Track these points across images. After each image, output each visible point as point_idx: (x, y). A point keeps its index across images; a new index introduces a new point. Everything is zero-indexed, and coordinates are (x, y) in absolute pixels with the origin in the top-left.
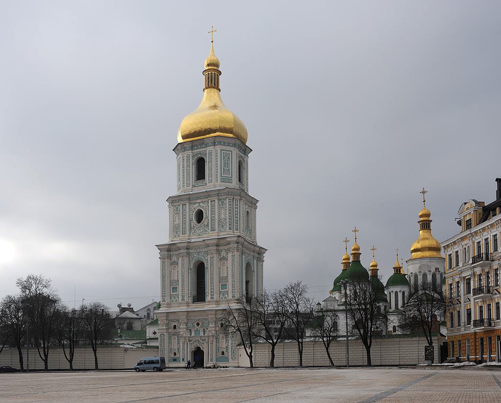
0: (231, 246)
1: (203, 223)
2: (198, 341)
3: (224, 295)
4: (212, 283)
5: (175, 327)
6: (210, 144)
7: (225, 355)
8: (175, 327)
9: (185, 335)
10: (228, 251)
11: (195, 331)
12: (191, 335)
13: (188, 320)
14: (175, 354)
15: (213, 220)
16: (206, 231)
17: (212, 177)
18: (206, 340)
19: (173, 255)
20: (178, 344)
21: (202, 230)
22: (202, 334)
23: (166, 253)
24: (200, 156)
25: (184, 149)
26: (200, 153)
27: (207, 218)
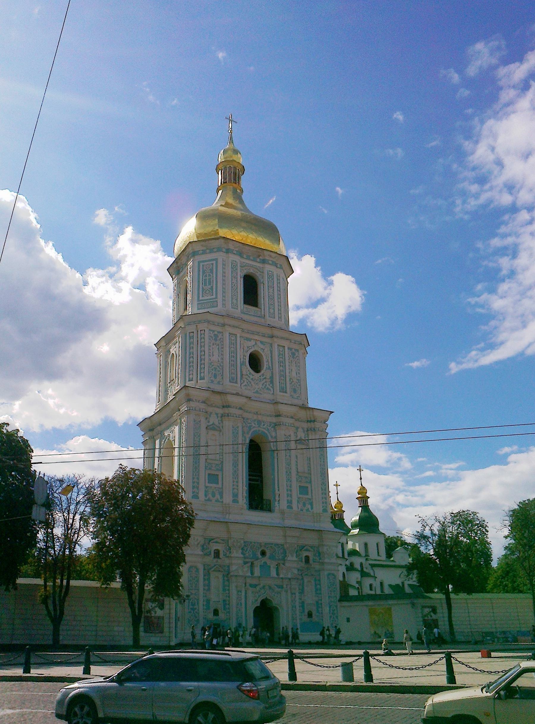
0: (317, 425)
1: (263, 375)
2: (270, 588)
3: (304, 504)
4: (289, 480)
5: (217, 554)
6: (271, 262)
7: (315, 618)
8: (217, 554)
9: (241, 574)
10: (314, 430)
11: (260, 566)
12: (252, 573)
13: (244, 542)
14: (216, 612)
15: (283, 376)
16: (268, 389)
17: (274, 309)
18: (282, 587)
19: (211, 413)
20: (224, 590)
21: (261, 386)
22: (274, 573)
23: (202, 406)
24: (252, 271)
25: (228, 251)
26: (252, 266)
27: (269, 368)
